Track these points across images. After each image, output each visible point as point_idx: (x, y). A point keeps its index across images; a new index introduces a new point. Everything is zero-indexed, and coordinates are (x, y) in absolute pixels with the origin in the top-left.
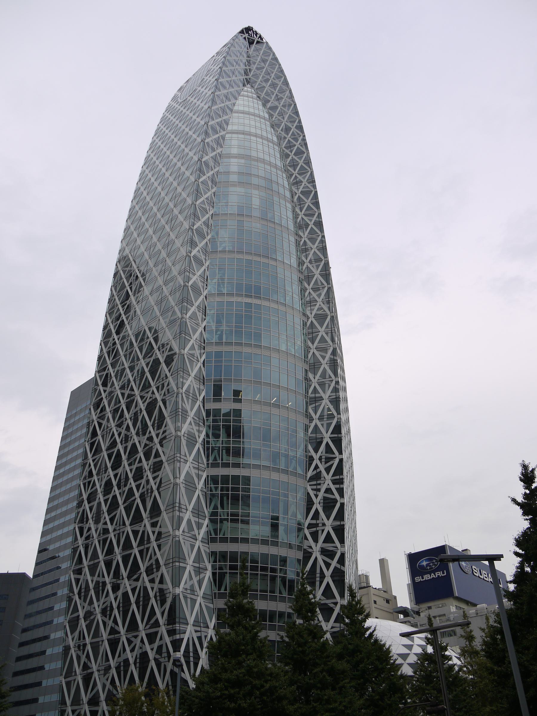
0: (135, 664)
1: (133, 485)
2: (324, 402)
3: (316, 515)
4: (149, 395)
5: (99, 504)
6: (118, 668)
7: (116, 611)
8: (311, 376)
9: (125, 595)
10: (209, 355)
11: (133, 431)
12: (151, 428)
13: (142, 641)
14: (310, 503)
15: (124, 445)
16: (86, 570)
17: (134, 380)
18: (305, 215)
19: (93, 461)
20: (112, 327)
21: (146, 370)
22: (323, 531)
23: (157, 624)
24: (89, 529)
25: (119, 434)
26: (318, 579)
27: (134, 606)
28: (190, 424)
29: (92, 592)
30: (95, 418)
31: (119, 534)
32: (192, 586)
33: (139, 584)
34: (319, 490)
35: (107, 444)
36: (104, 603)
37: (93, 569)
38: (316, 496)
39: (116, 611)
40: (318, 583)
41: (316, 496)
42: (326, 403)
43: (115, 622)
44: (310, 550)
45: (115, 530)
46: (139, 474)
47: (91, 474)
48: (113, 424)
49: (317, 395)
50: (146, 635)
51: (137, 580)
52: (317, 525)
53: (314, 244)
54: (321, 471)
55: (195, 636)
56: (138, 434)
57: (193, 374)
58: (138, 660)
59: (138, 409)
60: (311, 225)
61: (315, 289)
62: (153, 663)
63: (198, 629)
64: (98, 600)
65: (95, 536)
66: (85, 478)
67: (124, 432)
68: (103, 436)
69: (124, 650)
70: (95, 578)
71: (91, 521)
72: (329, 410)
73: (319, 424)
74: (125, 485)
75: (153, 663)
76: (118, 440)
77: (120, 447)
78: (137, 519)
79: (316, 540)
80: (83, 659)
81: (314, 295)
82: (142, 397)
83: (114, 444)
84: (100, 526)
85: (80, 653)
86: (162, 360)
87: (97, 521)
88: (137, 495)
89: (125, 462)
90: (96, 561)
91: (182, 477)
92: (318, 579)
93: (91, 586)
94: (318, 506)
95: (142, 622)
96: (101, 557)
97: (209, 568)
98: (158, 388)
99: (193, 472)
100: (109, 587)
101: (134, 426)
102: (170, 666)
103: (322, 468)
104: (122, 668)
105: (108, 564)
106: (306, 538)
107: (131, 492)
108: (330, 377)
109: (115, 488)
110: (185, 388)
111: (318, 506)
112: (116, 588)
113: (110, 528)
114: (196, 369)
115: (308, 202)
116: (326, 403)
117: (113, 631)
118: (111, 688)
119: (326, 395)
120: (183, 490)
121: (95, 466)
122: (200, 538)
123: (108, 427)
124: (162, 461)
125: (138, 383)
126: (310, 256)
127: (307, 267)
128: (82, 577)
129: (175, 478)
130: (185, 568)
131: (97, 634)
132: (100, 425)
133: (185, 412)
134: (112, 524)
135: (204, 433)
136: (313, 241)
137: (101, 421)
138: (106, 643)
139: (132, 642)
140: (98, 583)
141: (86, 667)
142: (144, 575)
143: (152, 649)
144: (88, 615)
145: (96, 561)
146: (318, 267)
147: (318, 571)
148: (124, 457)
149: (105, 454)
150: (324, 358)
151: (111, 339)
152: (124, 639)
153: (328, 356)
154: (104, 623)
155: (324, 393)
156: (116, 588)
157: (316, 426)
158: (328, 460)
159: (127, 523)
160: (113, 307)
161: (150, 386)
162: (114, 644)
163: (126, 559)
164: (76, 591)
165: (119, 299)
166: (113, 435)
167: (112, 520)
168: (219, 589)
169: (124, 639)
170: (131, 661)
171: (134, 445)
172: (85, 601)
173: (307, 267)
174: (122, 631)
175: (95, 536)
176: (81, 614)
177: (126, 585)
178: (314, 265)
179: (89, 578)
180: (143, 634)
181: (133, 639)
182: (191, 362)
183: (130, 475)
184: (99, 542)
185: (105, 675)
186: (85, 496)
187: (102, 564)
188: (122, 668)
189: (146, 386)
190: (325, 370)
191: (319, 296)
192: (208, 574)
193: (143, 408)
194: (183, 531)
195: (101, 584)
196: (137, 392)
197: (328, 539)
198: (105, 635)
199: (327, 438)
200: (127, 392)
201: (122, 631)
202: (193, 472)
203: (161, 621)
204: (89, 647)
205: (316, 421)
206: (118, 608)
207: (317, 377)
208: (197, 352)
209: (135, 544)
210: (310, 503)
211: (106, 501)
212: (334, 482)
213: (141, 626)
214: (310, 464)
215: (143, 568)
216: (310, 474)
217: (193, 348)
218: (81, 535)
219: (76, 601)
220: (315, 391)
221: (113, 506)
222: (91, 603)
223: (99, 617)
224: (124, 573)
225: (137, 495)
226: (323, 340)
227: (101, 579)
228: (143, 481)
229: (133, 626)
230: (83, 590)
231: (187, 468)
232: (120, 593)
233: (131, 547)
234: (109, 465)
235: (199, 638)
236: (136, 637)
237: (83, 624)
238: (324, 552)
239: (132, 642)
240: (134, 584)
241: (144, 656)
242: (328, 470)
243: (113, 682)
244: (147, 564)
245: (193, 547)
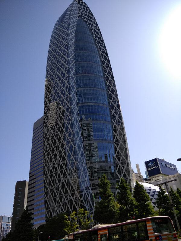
0: (68, 203)
1: (61, 149)
2: (117, 118)
3: (118, 152)
4: (63, 121)
5: (51, 156)
6: (63, 205)
7: (60, 188)
8: (112, 110)
9: (63, 183)
10: (80, 107)
11: (59, 133)
12: (64, 131)
13: (70, 196)
14: (116, 149)
15: (56, 137)
16: (49, 177)
17: (57, 117)
19: (47, 143)
20: (47, 101)
21: (60, 114)
22: (121, 157)
23: (74, 191)
24: (49, 164)
25: (54, 134)
26: (121, 172)
27: (66, 186)
28: (77, 129)
29: (52, 183)
30: (46, 130)
31: (58, 165)
32: (84, 178)
33: (67, 179)
34: (118, 145)
35: (51, 138)
36: (56, 186)
37: (51, 176)
38: (118, 147)
39: (60, 188)
40: (121, 173)
41: (118, 147)
42: (117, 118)
43: (60, 191)
44: (118, 163)
45: (57, 163)
46: (62, 146)
47: (47, 147)
48: (52, 131)
49: (114, 116)
50: (71, 194)
51: (66, 178)
52: (119, 155)
53: (108, 68)
54: (118, 139)
55: (86, 193)
56: (60, 134)
57: (75, 113)
58: (69, 202)
59: (59, 126)
60: (106, 62)
61: (110, 83)
62: (74, 203)
63: (86, 190)
64: (54, 185)
65: (51, 166)
66: (45, 149)
67: (56, 133)
68: (49, 135)
69: (64, 200)
70: (52, 179)
71: (49, 162)
72: (118, 120)
73: (116, 125)
74: (59, 150)
75: (74, 203)
76: (54, 136)
77: (55, 138)
78: (64, 159)
79: (119, 160)
80: (51, 204)
82: (60, 122)
83: (53, 137)
84: (52, 163)
85: (50, 202)
86: (65, 110)
87: (51, 161)
88: (63, 152)
89: (57, 143)
90: (52, 174)
91: (77, 145)
92: (121, 172)
93: (51, 181)
95: (69, 190)
96: (54, 172)
97: (88, 172)
98: (65, 119)
99: (80, 143)
100: (57, 181)
101: (59, 131)
102: (80, 203)
104: (64, 205)
105: (56, 174)
106: (116, 160)
107: (60, 152)
108: (118, 110)
109: (55, 151)
110: (74, 118)
112: (59, 181)
113: (56, 163)
114: (76, 112)
115: (104, 55)
116: (117, 118)
117: (60, 194)
118: (62, 211)
119: (117, 116)
120: (77, 149)
121: (48, 145)
122: (84, 163)
123: (50, 132)
124: (69, 141)
125: (58, 118)
127: (107, 76)
128: (48, 179)
129: (74, 145)
130: (81, 172)
131: (55, 196)
132: (48, 132)
133: (75, 125)
134: (56, 162)
135: (81, 131)
136: (107, 67)
137: (48, 131)
138: (58, 198)
139: (67, 197)
140: (53, 180)
141: (53, 206)
142: (68, 176)
143: (73, 198)
144: (51, 190)
145: (52, 174)
146: (110, 75)
147: (121, 169)
149: (50, 141)
150: (115, 104)
151: (47, 105)
152: (64, 196)
153: (116, 103)
154: (57, 192)
155: (116, 115)
156: (59, 181)
157: (115, 125)
159: (61, 161)
160: (47, 95)
161: (62, 118)
162: (61, 198)
163: (61, 172)
164: (47, 183)
165: (48, 92)
166: (52, 134)
167: (55, 161)
168: (92, 178)
169: (64, 196)
170: (67, 203)
171: (60, 137)
172: (50, 186)
173: (107, 76)
174: (63, 194)
175: (51, 166)
176: (49, 190)
177: (63, 180)
178: (109, 75)
179: (50, 179)
180: (70, 194)
181: (67, 196)
182: (74, 110)
183: (60, 146)
184: (52, 168)
185: (59, 208)
186: (46, 154)
187: (54, 174)
188: (64, 205)
189: (61, 118)
190: (116, 108)
191: (111, 85)
192: (88, 174)
193: (61, 126)
194: (79, 161)
195: (54, 181)
196: (58, 121)
198: (58, 196)
201: (63, 194)
202: (80, 143)
203: (75, 190)
204: (53, 200)
205: (115, 124)
206: (61, 187)
207: (114, 110)
208: (76, 106)
209: (64, 167)
210: (116, 149)
211: (53, 155)
212: (123, 142)
213: (69, 192)
214: (115, 137)
215: (67, 174)
216: (115, 140)
217: (74, 105)
218: (46, 167)
219: (47, 187)
220: (113, 115)
222: (52, 186)
223: (55, 190)
224: (62, 176)
225: (63, 152)
227: (54, 179)
228: (64, 148)
229: (66, 192)
230: (49, 183)
231: (78, 142)
232: (61, 182)
233: (63, 168)
234: (52, 144)
235: (87, 193)
236: (68, 195)
237: (50, 193)
238: (122, 163)
239: (67, 197)
240: (65, 179)
241: (71, 200)
243: (62, 210)
244: (68, 173)
245: (82, 166)
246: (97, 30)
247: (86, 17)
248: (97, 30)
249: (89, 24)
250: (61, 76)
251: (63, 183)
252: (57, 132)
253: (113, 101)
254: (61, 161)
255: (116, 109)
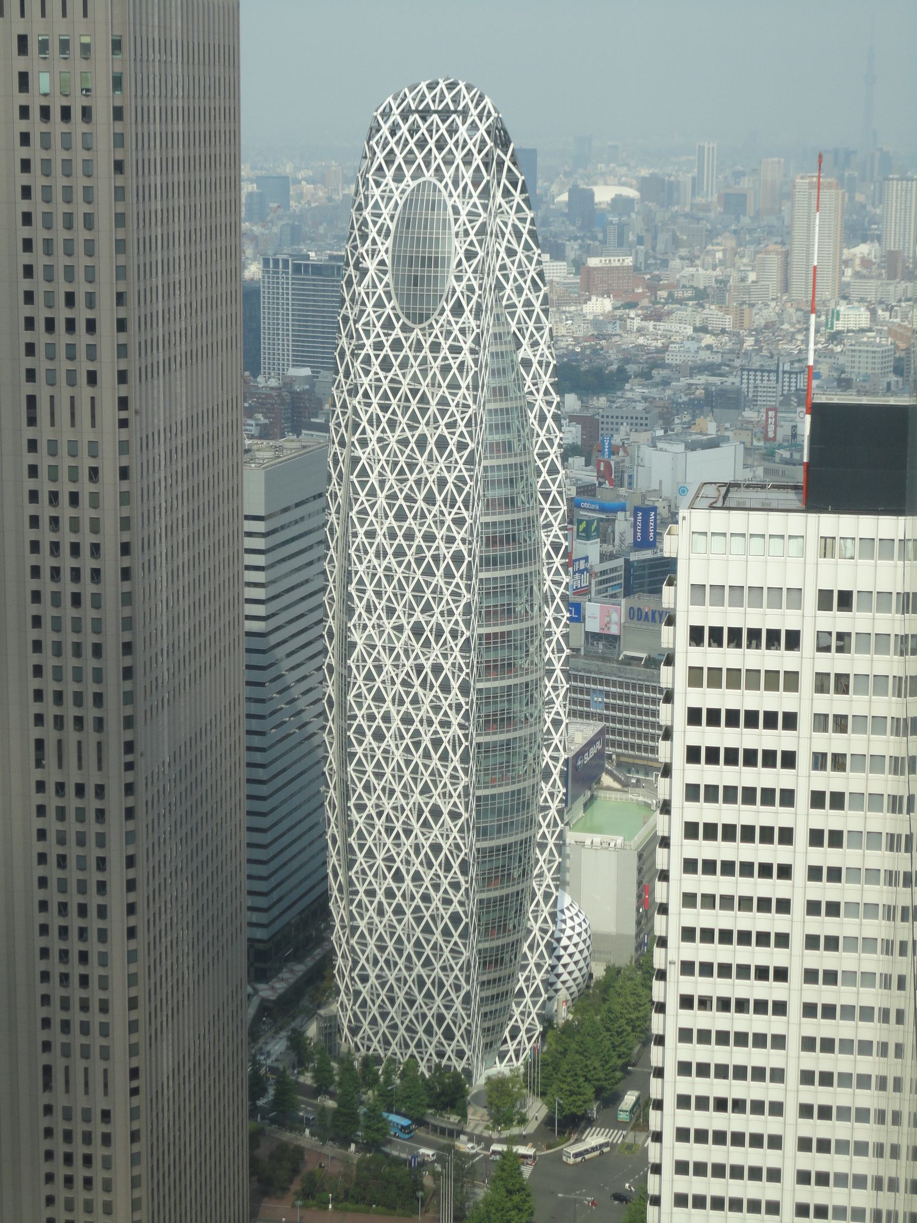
5: (380, 904)
7: (410, 983)
8: (543, 784)
18: (554, 582)
42: (553, 812)
47: (364, 872)
67: (403, 855)
77: (398, 864)
78: (427, 930)
81: (553, 695)
84: (385, 920)
94: (539, 897)
103: (545, 868)
111: (539, 897)
112: (409, 969)
116: (553, 812)
126: (554, 644)
148: (408, 879)
149: (379, 862)
158: (550, 862)
177: (419, 969)
197: (545, 921)
199: (551, 842)
200: (402, 818)
221: (399, 911)
226: (556, 749)
232: (414, 974)
242: (549, 870)
246: (550, 421)
247: (520, 311)
248: (550, 421)
249: (527, 363)
250: (430, 676)
251: (420, 977)
252: (407, 852)
253: (552, 758)
254: (418, 930)
255: (553, 785)
